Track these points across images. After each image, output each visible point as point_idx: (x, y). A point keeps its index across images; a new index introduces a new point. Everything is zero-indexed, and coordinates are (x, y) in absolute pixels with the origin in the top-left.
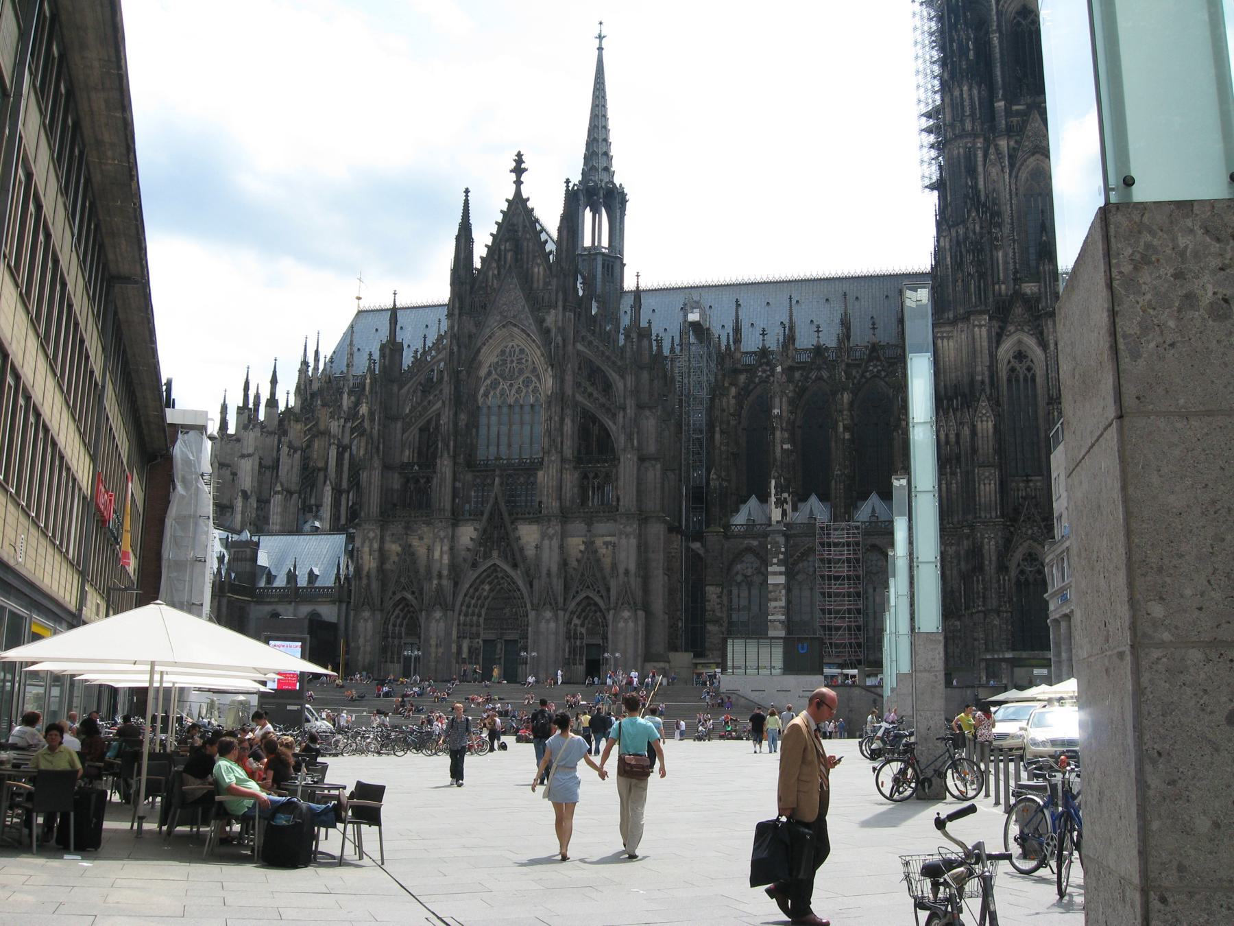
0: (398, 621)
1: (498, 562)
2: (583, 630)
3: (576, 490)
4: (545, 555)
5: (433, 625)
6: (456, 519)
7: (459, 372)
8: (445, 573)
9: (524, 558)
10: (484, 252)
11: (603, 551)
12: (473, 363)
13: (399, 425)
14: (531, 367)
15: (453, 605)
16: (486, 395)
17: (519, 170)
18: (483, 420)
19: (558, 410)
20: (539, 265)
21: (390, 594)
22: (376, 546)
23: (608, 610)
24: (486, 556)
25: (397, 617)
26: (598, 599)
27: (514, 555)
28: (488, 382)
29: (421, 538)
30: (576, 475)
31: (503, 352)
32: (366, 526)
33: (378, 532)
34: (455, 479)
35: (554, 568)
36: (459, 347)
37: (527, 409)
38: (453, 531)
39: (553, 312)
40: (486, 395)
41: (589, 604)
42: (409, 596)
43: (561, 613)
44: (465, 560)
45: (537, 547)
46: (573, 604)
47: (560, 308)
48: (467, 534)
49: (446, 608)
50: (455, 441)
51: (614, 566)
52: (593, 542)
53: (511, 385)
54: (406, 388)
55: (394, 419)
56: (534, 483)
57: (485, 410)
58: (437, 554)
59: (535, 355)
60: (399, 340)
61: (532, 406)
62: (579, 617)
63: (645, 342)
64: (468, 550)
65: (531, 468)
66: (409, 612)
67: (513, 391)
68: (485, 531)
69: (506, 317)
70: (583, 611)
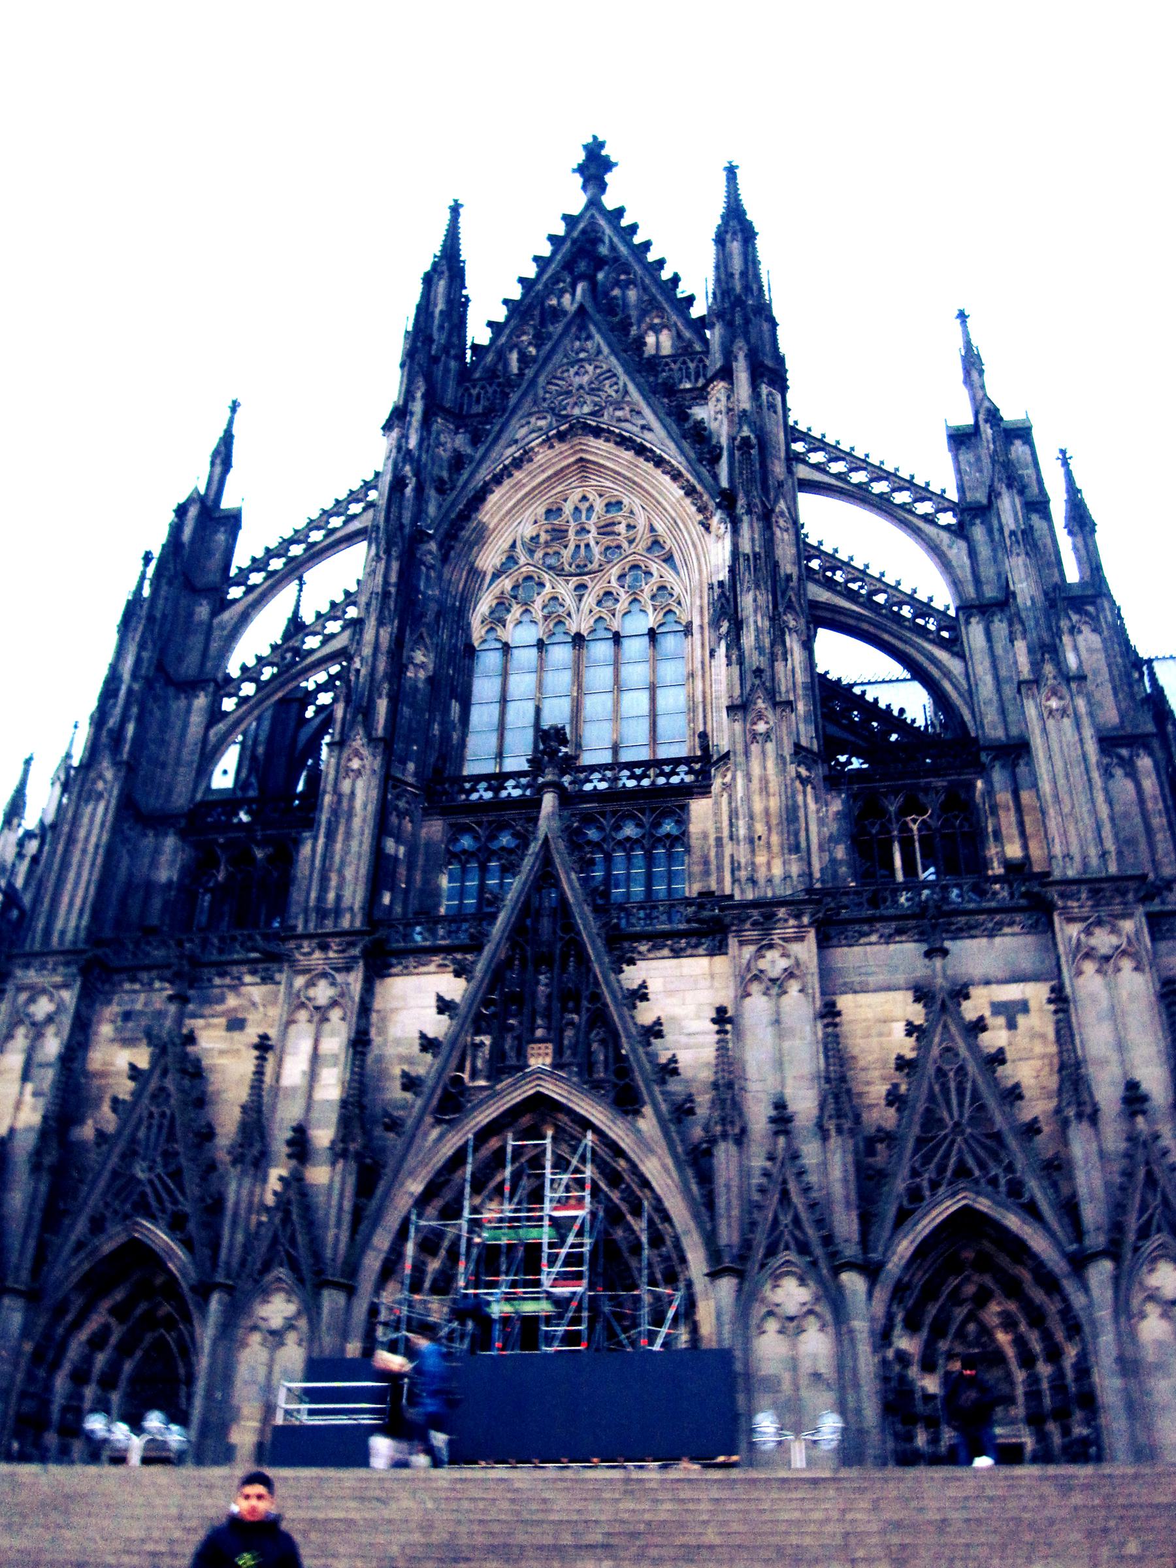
0: (101, 1359)
1: (553, 1090)
2: (931, 1384)
3: (840, 852)
4: (757, 1052)
5: (252, 1356)
6: (380, 952)
7: (419, 536)
8: (323, 1136)
9: (670, 1070)
10: (500, 314)
11: (995, 1037)
12: (460, 528)
13: (201, 701)
14: (641, 546)
15: (352, 1268)
16: (497, 619)
17: (595, 166)
18: (484, 688)
19: (764, 598)
20: (656, 330)
21: (81, 1226)
22: (52, 1046)
23: (1079, 1262)
24: (504, 1065)
25: (97, 1342)
26: (1013, 1221)
27: (622, 1065)
28: (506, 584)
29: (236, 1024)
30: (836, 806)
31: (552, 512)
32: (31, 976)
33: (68, 997)
34: (382, 827)
35: (804, 1103)
36: (419, 489)
37: (635, 647)
38: (368, 990)
39: (719, 389)
40: (497, 619)
41: (954, 1266)
42: (159, 1236)
43: (853, 1282)
44: (410, 1083)
45: (721, 1017)
46: (905, 1247)
47: (742, 376)
48: (419, 1002)
49: (315, 1278)
50: (393, 712)
51: (1072, 1074)
52: (961, 992)
53: (582, 587)
54: (238, 608)
55: (190, 687)
56: (681, 838)
57: (489, 660)
58: (294, 1070)
59: (661, 501)
60: (227, 503)
61: (652, 635)
62: (912, 1326)
63: (1018, 449)
64: (428, 1044)
65: (656, 800)
66: (150, 1321)
67: (590, 600)
68: (497, 974)
69: (567, 416)
70: (930, 1292)
